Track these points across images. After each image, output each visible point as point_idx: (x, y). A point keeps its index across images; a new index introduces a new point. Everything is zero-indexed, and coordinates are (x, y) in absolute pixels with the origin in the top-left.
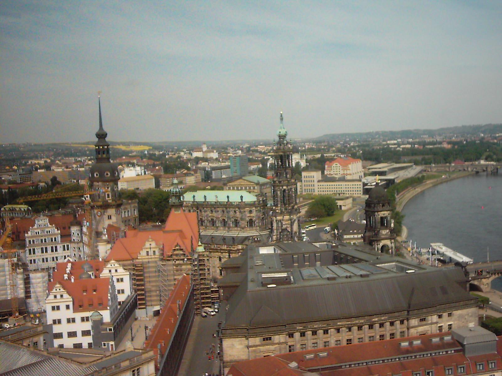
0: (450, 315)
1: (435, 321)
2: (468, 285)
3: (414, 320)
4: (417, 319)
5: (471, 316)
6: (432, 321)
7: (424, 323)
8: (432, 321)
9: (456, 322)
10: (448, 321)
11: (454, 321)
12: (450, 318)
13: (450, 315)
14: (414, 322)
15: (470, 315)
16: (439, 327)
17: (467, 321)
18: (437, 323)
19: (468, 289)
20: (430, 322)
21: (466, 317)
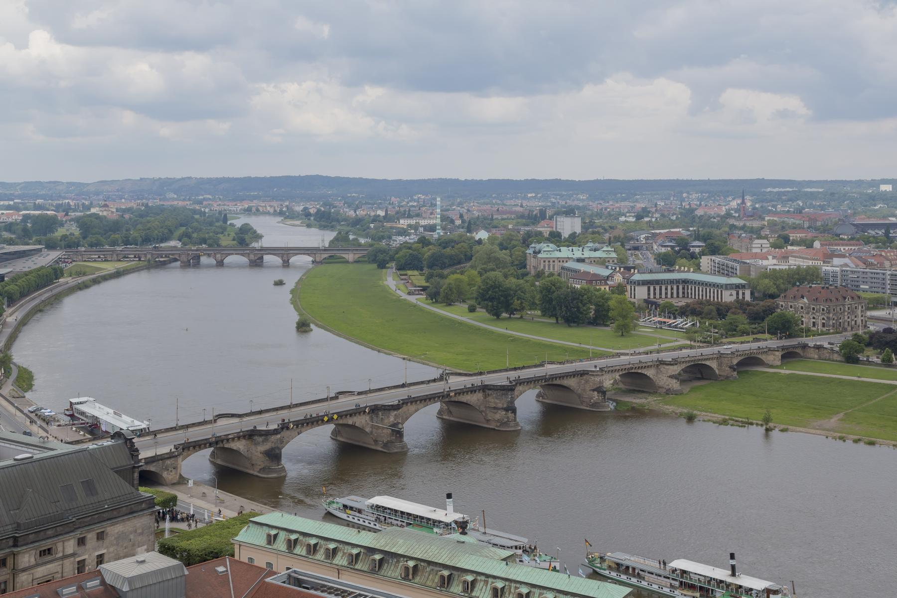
0: (100, 536)
1: (70, 550)
2: (136, 475)
3: (27, 556)
4: (33, 552)
5: (142, 534)
6: (63, 552)
7: (49, 558)
8: (63, 552)
9: (111, 549)
10: (95, 549)
11: (107, 548)
12: (100, 542)
13: (100, 536)
14: (27, 558)
15: (139, 531)
16: (79, 562)
17: (133, 545)
18: (74, 555)
19: (136, 482)
20: (60, 555)
21: (132, 537)
